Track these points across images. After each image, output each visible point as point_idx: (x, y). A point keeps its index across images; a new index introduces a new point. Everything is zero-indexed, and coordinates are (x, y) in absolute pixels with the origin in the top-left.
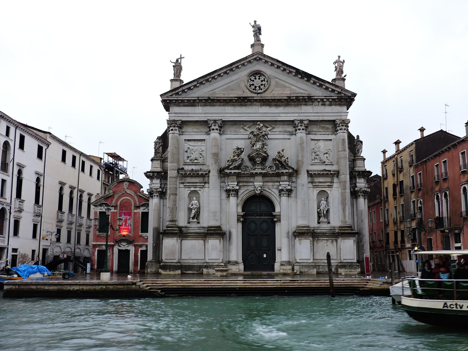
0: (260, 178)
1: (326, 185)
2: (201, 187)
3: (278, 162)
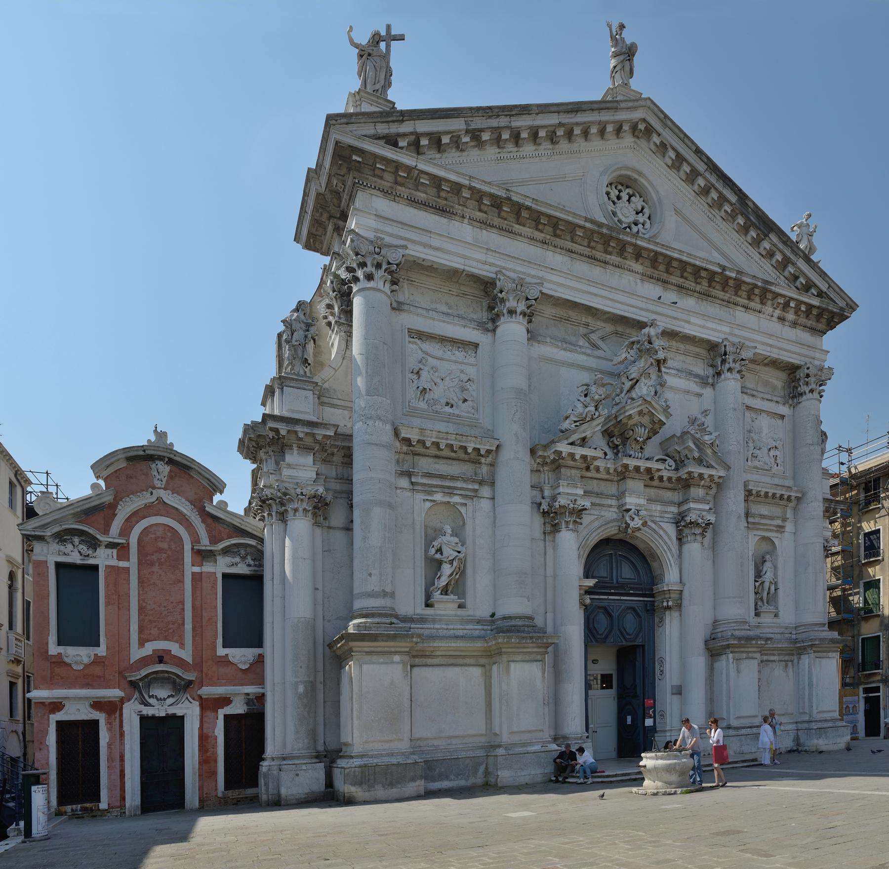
0: (635, 485)
1: (774, 526)
2: (469, 493)
3: (695, 444)
